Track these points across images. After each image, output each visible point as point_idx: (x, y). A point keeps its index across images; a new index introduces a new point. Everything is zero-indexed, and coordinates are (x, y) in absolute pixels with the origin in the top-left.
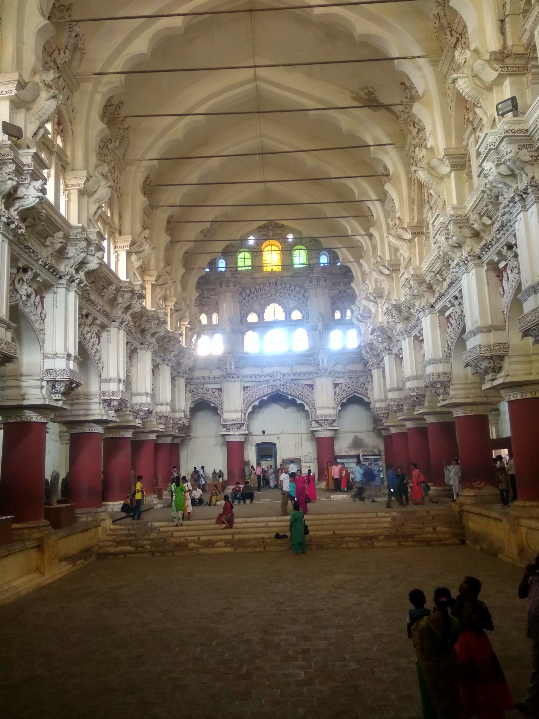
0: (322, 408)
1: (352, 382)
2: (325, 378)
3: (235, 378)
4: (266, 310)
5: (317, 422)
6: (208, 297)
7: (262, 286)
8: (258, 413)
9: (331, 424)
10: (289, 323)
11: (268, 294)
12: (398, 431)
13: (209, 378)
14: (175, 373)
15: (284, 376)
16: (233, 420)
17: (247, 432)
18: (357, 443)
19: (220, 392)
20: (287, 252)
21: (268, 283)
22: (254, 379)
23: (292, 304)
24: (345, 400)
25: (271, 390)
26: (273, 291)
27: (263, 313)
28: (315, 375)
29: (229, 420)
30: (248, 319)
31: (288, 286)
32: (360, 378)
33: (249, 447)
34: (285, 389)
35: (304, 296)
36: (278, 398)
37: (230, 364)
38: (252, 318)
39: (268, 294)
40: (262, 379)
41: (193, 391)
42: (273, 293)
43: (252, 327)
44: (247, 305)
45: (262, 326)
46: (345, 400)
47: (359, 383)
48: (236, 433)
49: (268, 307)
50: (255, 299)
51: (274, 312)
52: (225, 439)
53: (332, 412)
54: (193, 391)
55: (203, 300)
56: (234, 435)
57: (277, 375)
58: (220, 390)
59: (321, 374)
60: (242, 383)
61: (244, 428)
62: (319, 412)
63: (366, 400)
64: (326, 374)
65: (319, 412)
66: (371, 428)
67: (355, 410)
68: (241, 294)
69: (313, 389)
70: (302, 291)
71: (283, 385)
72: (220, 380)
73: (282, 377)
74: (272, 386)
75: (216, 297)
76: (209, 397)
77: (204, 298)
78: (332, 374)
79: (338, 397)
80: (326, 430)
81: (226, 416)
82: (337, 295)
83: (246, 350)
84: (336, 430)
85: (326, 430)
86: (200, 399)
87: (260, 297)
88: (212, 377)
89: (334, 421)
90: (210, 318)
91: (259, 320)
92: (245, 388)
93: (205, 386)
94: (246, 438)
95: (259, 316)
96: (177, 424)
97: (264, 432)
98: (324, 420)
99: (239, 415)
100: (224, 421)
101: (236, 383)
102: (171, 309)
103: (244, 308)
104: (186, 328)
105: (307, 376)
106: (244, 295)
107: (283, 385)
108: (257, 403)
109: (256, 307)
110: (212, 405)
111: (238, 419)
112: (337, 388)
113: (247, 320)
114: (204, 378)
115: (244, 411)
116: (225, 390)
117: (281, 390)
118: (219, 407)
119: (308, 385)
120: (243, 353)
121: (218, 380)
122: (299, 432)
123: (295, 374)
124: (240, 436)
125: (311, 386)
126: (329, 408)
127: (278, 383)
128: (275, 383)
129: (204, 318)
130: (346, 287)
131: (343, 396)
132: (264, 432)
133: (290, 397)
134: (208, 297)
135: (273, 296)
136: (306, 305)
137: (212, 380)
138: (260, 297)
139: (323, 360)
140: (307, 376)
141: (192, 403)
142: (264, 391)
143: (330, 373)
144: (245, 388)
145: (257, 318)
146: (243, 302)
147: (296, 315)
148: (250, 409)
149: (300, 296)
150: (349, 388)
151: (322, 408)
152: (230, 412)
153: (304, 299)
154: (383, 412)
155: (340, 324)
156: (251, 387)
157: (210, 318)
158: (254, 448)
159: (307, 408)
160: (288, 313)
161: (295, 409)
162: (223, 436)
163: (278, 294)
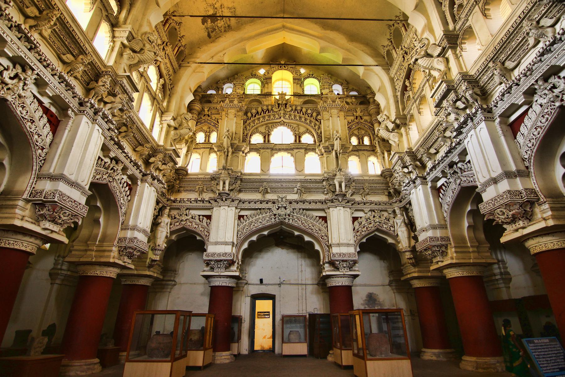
0: (339, 245)
1: (374, 217)
2: (342, 208)
3: (228, 202)
4: (272, 133)
5: (332, 263)
6: (209, 116)
7: (270, 108)
8: (257, 258)
9: (350, 268)
11: (277, 116)
12: (465, 274)
13: (196, 201)
15: (290, 203)
16: (219, 255)
17: (237, 274)
18: (371, 298)
19: (209, 221)
20: (298, 81)
21: (277, 105)
22: (252, 206)
24: (364, 240)
25: (273, 220)
26: (282, 112)
27: (269, 135)
28: (330, 204)
29: (213, 254)
30: (251, 140)
31: (299, 108)
32: (383, 213)
33: (243, 297)
34: (291, 221)
35: (316, 120)
37: (224, 183)
38: (257, 139)
39: (277, 116)
40: (264, 206)
41: (175, 218)
42: (282, 115)
43: (255, 148)
44: (252, 124)
45: (268, 149)
46: (364, 240)
47: (383, 218)
48: (222, 274)
50: (261, 119)
51: (282, 135)
53: (352, 250)
54: (175, 218)
55: (203, 118)
56: (220, 276)
57: (282, 201)
58: (209, 217)
59: (337, 203)
60: (238, 211)
61: (234, 268)
62: (335, 250)
63: (390, 241)
64: (343, 203)
65: (335, 250)
66: (387, 281)
68: (246, 114)
69: (326, 222)
70: (315, 114)
71: (289, 215)
72: (210, 205)
73: (288, 203)
74: (275, 215)
75: (217, 116)
76: (195, 226)
77: (205, 115)
78: (350, 204)
79: (358, 234)
80: (344, 276)
81: (211, 249)
82: (352, 121)
84: (355, 276)
85: (344, 276)
86: (183, 229)
87: (267, 117)
88: (199, 199)
89: (355, 262)
90: (208, 136)
91: (265, 141)
92: (240, 217)
93: (191, 211)
94: (237, 284)
95: (265, 137)
96: (125, 248)
97: (261, 281)
98: (343, 261)
99: (228, 249)
100: (208, 256)
101: (230, 208)
102: (122, 43)
103: (248, 128)
104: (169, 126)
105: (319, 206)
106: (249, 115)
107: (289, 215)
108: (254, 238)
110: (198, 238)
111: (226, 253)
112: (356, 223)
113: (250, 141)
114: (190, 200)
115: (238, 246)
117: (287, 221)
118: (206, 239)
119: (320, 217)
120: (241, 174)
121: (208, 205)
122: (304, 283)
123: (304, 202)
124: (228, 279)
125: (325, 219)
126: (348, 245)
127: (282, 212)
128: (279, 211)
129: (200, 137)
130: (362, 113)
131: (363, 233)
132: (261, 281)
133: (296, 233)
134: (209, 116)
135: (282, 119)
136: (319, 128)
137: (201, 204)
138: (267, 117)
139: (340, 186)
140: (319, 206)
142: (264, 220)
143: (348, 202)
144: (240, 217)
146: (248, 122)
148: (245, 246)
149: (312, 119)
150: (370, 224)
151: (339, 245)
152: (217, 243)
153: (316, 122)
154: (439, 243)
155: (358, 151)
156: (249, 216)
157: (208, 136)
158: (248, 300)
159: (317, 247)
160: (297, 137)
161: (299, 255)
162: (207, 277)
163: (287, 116)
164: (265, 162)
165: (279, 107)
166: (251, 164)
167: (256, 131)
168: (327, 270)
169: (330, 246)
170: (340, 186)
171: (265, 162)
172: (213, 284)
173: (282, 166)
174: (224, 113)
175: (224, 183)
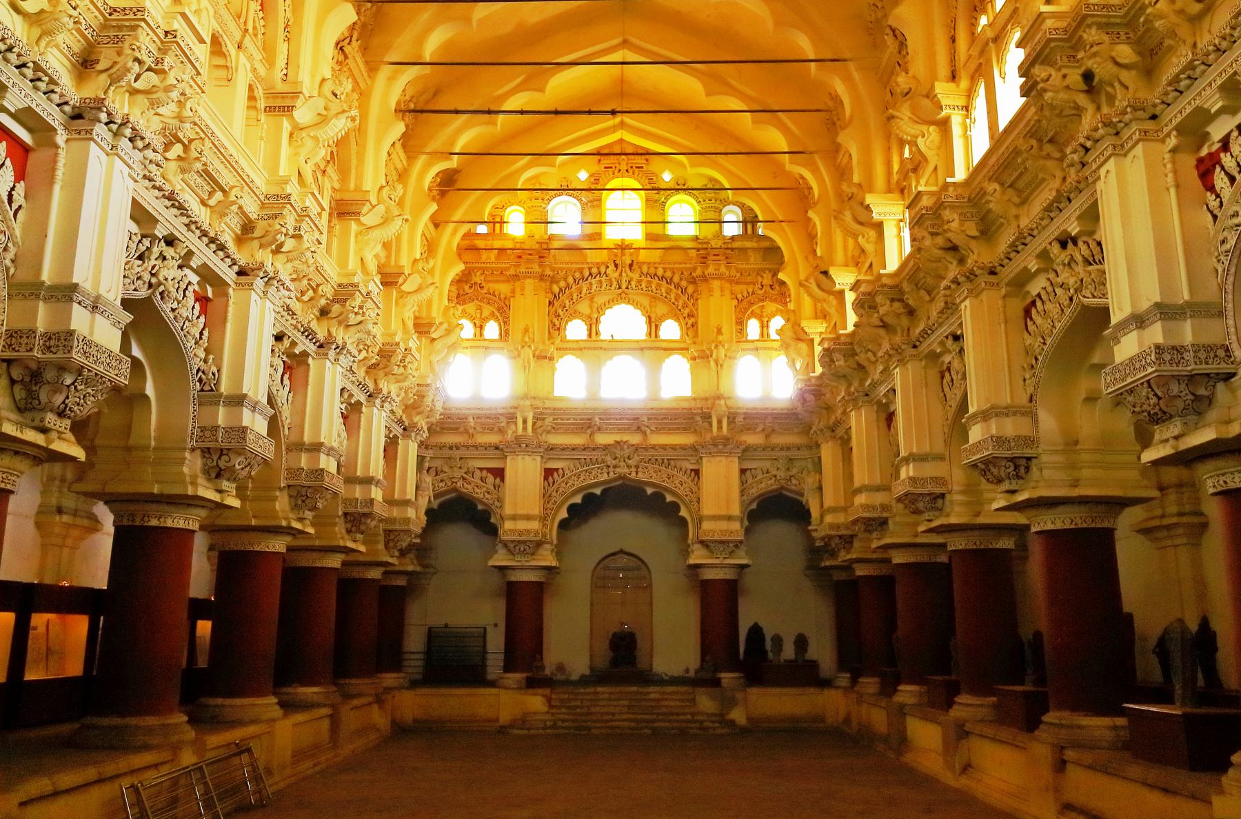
10: (653, 348)
14: (398, 430)
23: (661, 309)
36: (624, 496)
37: (525, 422)
38: (576, 330)
43: (578, 348)
45: (596, 348)
49: (608, 311)
51: (624, 321)
52: (504, 576)
56: (522, 568)
67: (780, 532)
83: (557, 393)
91: (590, 335)
116: (508, 473)
139: (720, 422)
141: (436, 496)
145: (586, 333)
147: (671, 330)
165: (616, 266)
166: (570, 382)
167: (575, 315)
168: (697, 556)
169: (700, 520)
170: (720, 422)
172: (513, 579)
174: (518, 284)
175: (525, 422)
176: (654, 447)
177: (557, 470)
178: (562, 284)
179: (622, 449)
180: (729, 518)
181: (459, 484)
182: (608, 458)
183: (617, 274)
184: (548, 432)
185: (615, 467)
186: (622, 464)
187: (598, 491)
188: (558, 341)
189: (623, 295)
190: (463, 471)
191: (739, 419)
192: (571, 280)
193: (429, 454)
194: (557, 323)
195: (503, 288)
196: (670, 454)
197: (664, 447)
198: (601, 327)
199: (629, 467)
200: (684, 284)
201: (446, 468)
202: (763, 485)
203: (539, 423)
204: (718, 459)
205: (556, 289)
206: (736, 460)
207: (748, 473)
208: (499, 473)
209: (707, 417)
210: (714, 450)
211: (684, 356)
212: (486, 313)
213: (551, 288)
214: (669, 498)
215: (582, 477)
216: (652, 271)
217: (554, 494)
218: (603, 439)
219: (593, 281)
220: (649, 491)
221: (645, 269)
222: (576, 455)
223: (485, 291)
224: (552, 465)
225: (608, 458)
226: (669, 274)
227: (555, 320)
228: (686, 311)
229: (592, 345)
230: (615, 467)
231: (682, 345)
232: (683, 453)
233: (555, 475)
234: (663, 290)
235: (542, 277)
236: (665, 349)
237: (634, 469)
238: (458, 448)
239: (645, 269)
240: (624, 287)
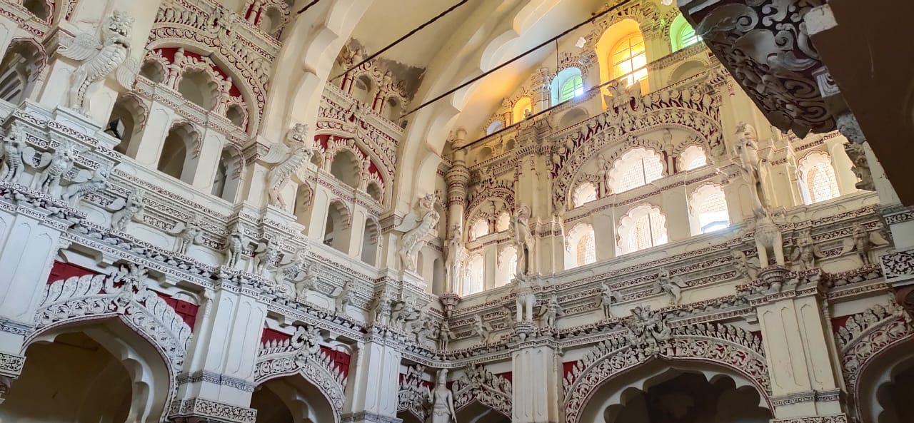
38: (585, 195)
43: (586, 215)
45: (610, 208)
49: (617, 164)
51: (636, 169)
109: (591, 168)
147: (694, 159)
164: (607, 239)
166: (580, 250)
170: (770, 253)
171: (607, 239)
173: (643, 234)
176: (684, 309)
177: (575, 363)
178: (562, 150)
179: (641, 319)
180: (816, 397)
181: (478, 397)
182: (630, 336)
183: (618, 120)
184: (558, 316)
185: (643, 346)
186: (650, 340)
187: (639, 385)
188: (562, 212)
189: (632, 140)
190: (482, 380)
191: (805, 239)
192: (570, 144)
193: (448, 364)
194: (561, 193)
195: (510, 177)
196: (714, 313)
197: (700, 306)
198: (610, 183)
199: (659, 343)
200: (696, 97)
201: (465, 380)
202: (884, 337)
203: (544, 308)
204: (779, 305)
205: (557, 159)
206: (813, 302)
207: (850, 324)
208: (508, 376)
209: (750, 251)
210: (767, 293)
211: (714, 182)
212: (499, 206)
213: (552, 160)
214: (740, 383)
215: (606, 367)
216: (656, 99)
217: (575, 394)
218: (620, 312)
219: (594, 137)
220: (709, 375)
221: (648, 102)
222: (591, 338)
223: (495, 185)
224: (569, 357)
225: (630, 336)
226: (675, 95)
227: (559, 190)
228: (706, 129)
229: (602, 203)
230: (643, 346)
231: (709, 171)
232: (733, 309)
233: (574, 368)
234: (674, 115)
235: (540, 153)
236: (688, 183)
237: (668, 345)
238: (471, 355)
239: (648, 102)
240: (627, 129)
